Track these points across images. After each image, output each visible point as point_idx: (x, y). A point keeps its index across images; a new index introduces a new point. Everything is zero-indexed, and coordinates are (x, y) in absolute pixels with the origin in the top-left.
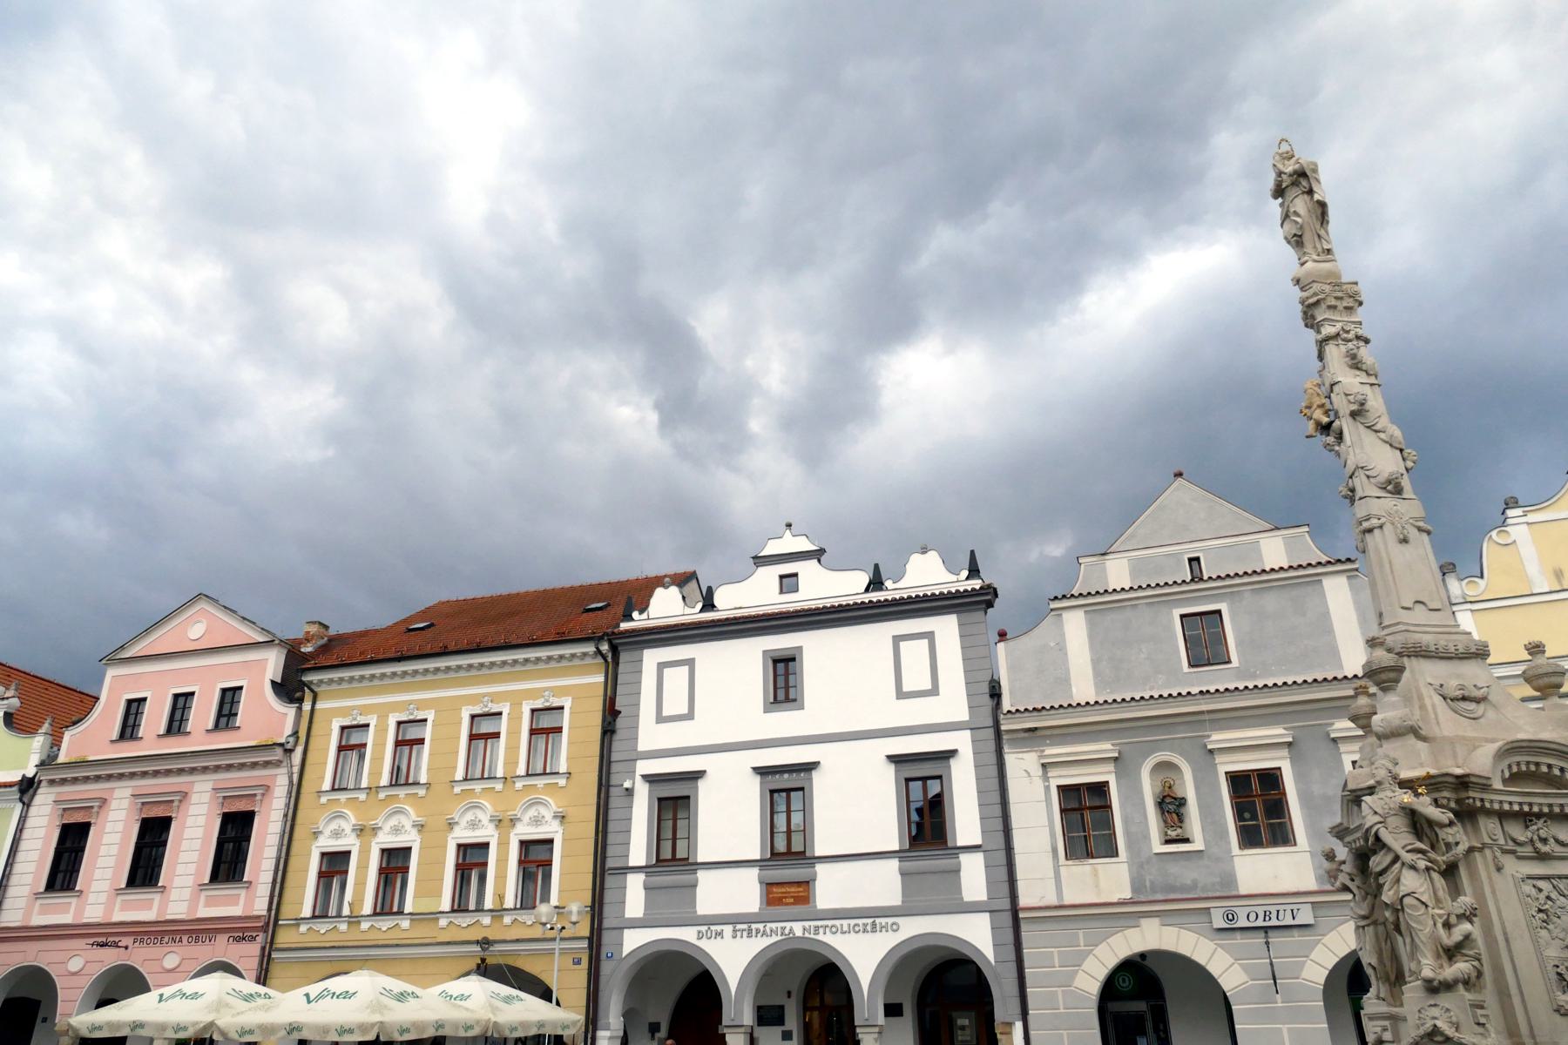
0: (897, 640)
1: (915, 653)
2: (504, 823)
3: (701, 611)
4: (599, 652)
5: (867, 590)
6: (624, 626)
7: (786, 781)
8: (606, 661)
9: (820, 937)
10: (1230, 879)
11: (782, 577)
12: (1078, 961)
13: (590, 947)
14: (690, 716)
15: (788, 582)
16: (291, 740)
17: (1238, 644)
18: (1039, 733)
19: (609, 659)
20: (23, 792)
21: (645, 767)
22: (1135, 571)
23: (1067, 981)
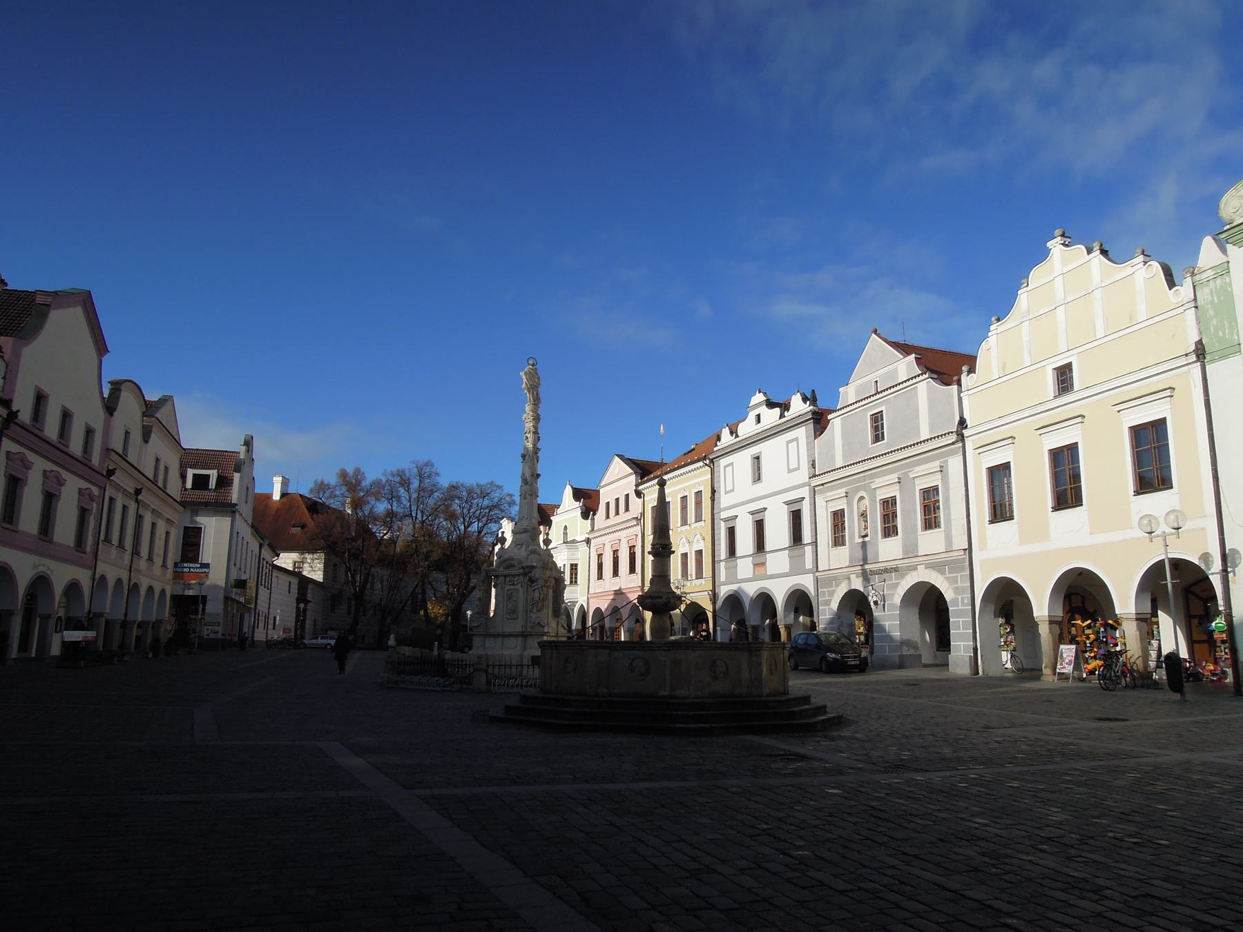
0: (788, 442)
3: (735, 438)
4: (706, 464)
5: (780, 418)
6: (715, 449)
7: (758, 517)
8: (710, 467)
12: (832, 593)
14: (732, 490)
15: (758, 420)
16: (639, 515)
17: (888, 429)
18: (825, 486)
20: (587, 543)
21: (724, 515)
23: (828, 603)
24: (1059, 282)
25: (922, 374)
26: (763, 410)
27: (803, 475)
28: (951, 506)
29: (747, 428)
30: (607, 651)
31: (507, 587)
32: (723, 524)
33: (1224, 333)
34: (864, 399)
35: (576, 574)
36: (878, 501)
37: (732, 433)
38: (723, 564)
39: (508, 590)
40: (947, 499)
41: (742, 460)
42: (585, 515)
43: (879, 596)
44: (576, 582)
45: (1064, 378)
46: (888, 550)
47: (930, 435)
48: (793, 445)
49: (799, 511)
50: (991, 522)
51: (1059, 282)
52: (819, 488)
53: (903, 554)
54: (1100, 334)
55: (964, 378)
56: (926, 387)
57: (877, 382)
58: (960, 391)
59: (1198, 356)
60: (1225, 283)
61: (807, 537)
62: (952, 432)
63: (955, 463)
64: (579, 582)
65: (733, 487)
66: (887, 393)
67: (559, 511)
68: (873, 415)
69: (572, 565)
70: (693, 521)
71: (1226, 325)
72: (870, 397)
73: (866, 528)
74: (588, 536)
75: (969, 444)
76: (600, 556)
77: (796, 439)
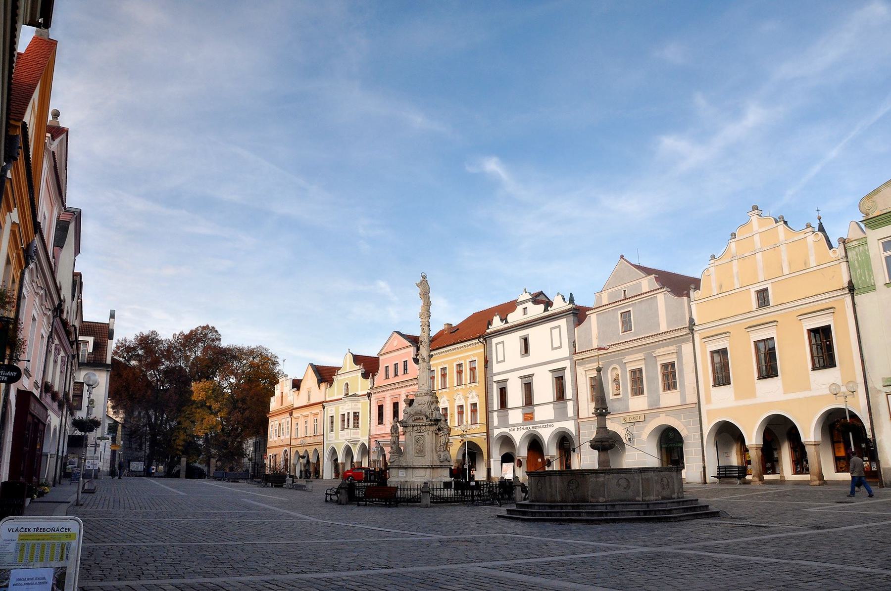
0: (552, 329)
1: (556, 332)
2: (466, 398)
4: (480, 342)
5: (544, 312)
6: (488, 331)
9: (536, 430)
10: (628, 407)
11: (524, 309)
13: (487, 434)
14: (504, 361)
18: (584, 360)
19: (485, 343)
20: (368, 397)
21: (496, 378)
22: (610, 297)
24: (757, 238)
25: (661, 288)
26: (530, 305)
27: (565, 352)
28: (685, 375)
29: (515, 317)
30: (603, 475)
31: (414, 434)
32: (495, 385)
33: (865, 278)
34: (616, 302)
35: (358, 420)
36: (628, 371)
37: (502, 320)
38: (495, 414)
39: (415, 436)
40: (681, 371)
41: (513, 341)
42: (365, 376)
43: (631, 435)
44: (358, 426)
45: (763, 297)
46: (638, 404)
47: (668, 328)
48: (556, 332)
49: (562, 377)
50: (714, 386)
51: (757, 238)
52: (579, 361)
53: (649, 406)
54: (786, 271)
55: (692, 293)
56: (663, 299)
57: (625, 291)
58: (690, 301)
59: (849, 291)
60: (865, 249)
61: (569, 394)
62: (686, 328)
63: (687, 348)
64: (360, 426)
65: (504, 358)
66: (633, 299)
67: (340, 372)
68: (622, 313)
69: (355, 413)
70: (468, 382)
71: (867, 273)
72: (621, 301)
73: (618, 388)
74: (369, 391)
75: (697, 337)
76: (381, 408)
77: (559, 327)
